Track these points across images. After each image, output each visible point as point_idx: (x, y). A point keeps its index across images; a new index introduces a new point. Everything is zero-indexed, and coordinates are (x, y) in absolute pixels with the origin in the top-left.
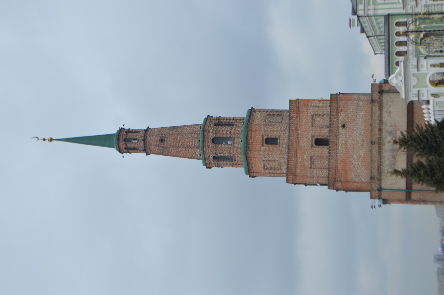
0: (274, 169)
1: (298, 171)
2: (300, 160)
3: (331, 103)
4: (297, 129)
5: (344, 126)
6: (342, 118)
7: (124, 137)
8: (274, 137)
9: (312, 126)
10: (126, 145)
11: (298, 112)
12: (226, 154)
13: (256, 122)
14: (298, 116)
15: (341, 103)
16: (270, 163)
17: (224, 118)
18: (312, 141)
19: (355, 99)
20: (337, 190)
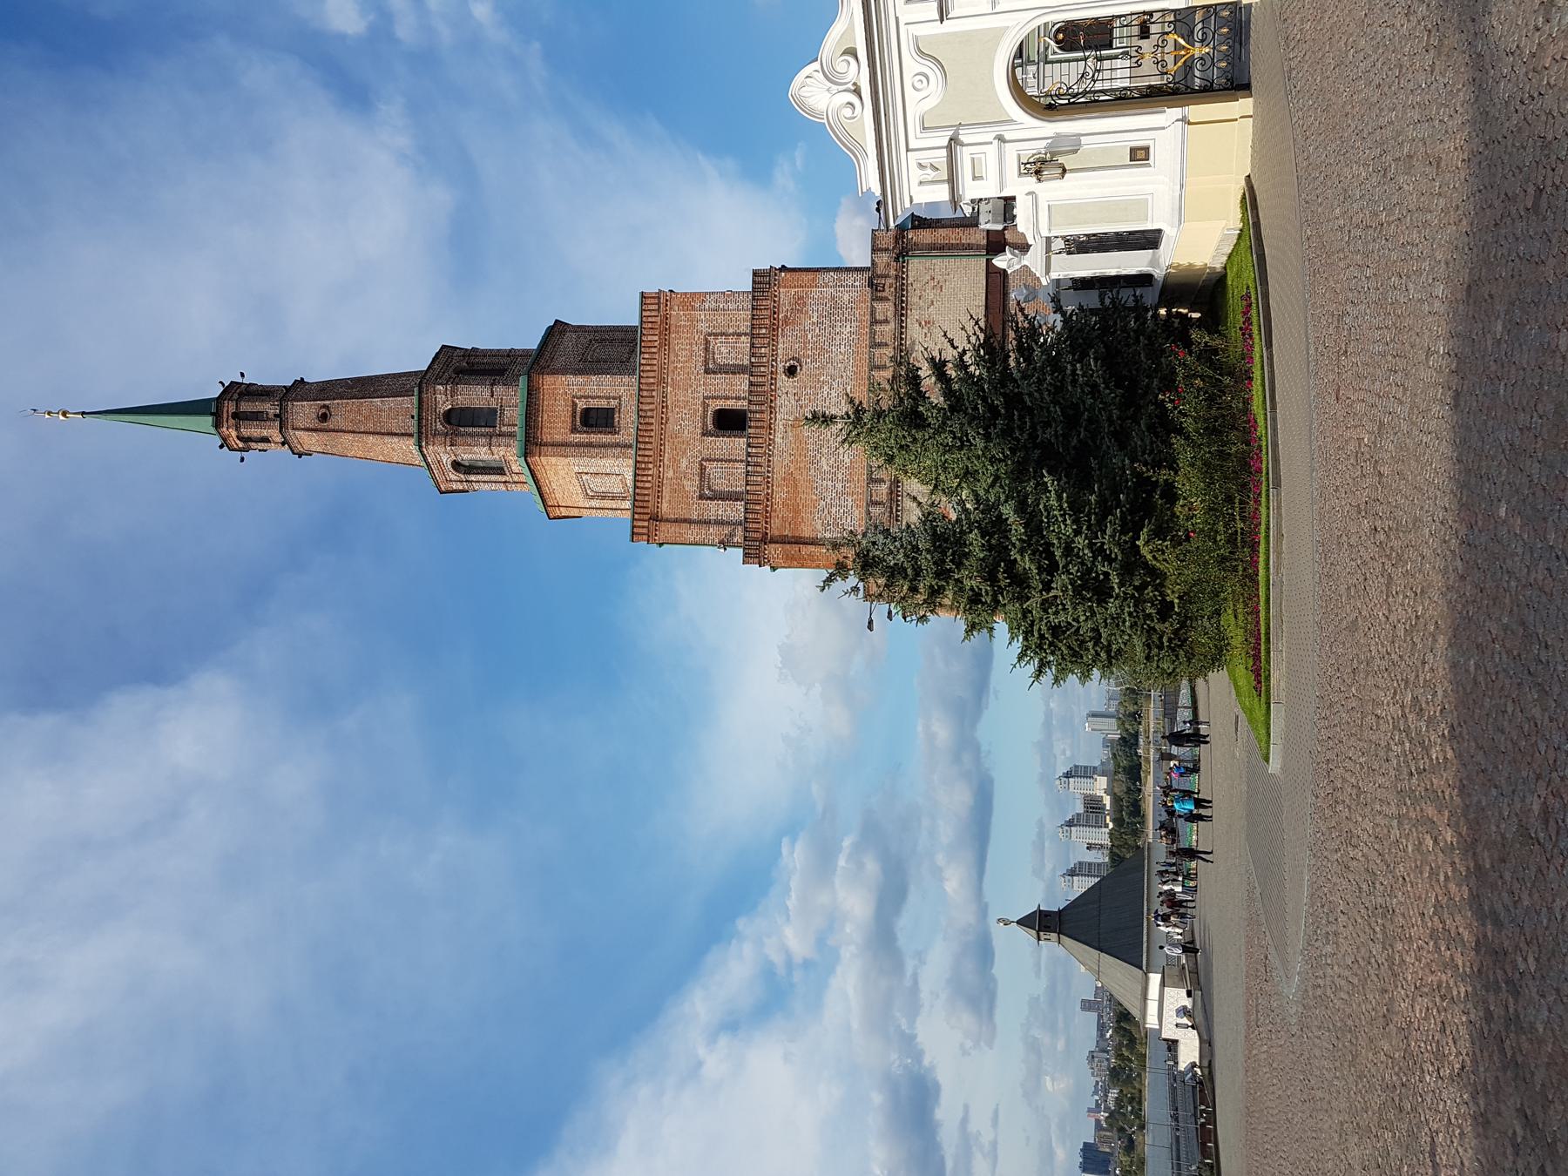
0: (613, 498)
1: (665, 505)
2: (670, 474)
3: (754, 298)
4: (662, 381)
5: (791, 371)
6: (785, 347)
7: (232, 409)
8: (603, 404)
9: (707, 371)
10: (237, 429)
11: (665, 329)
12: (480, 453)
13: (560, 362)
14: (665, 343)
15: (785, 295)
16: (598, 480)
17: (485, 353)
18: (704, 417)
19: (826, 286)
20: (774, 569)
